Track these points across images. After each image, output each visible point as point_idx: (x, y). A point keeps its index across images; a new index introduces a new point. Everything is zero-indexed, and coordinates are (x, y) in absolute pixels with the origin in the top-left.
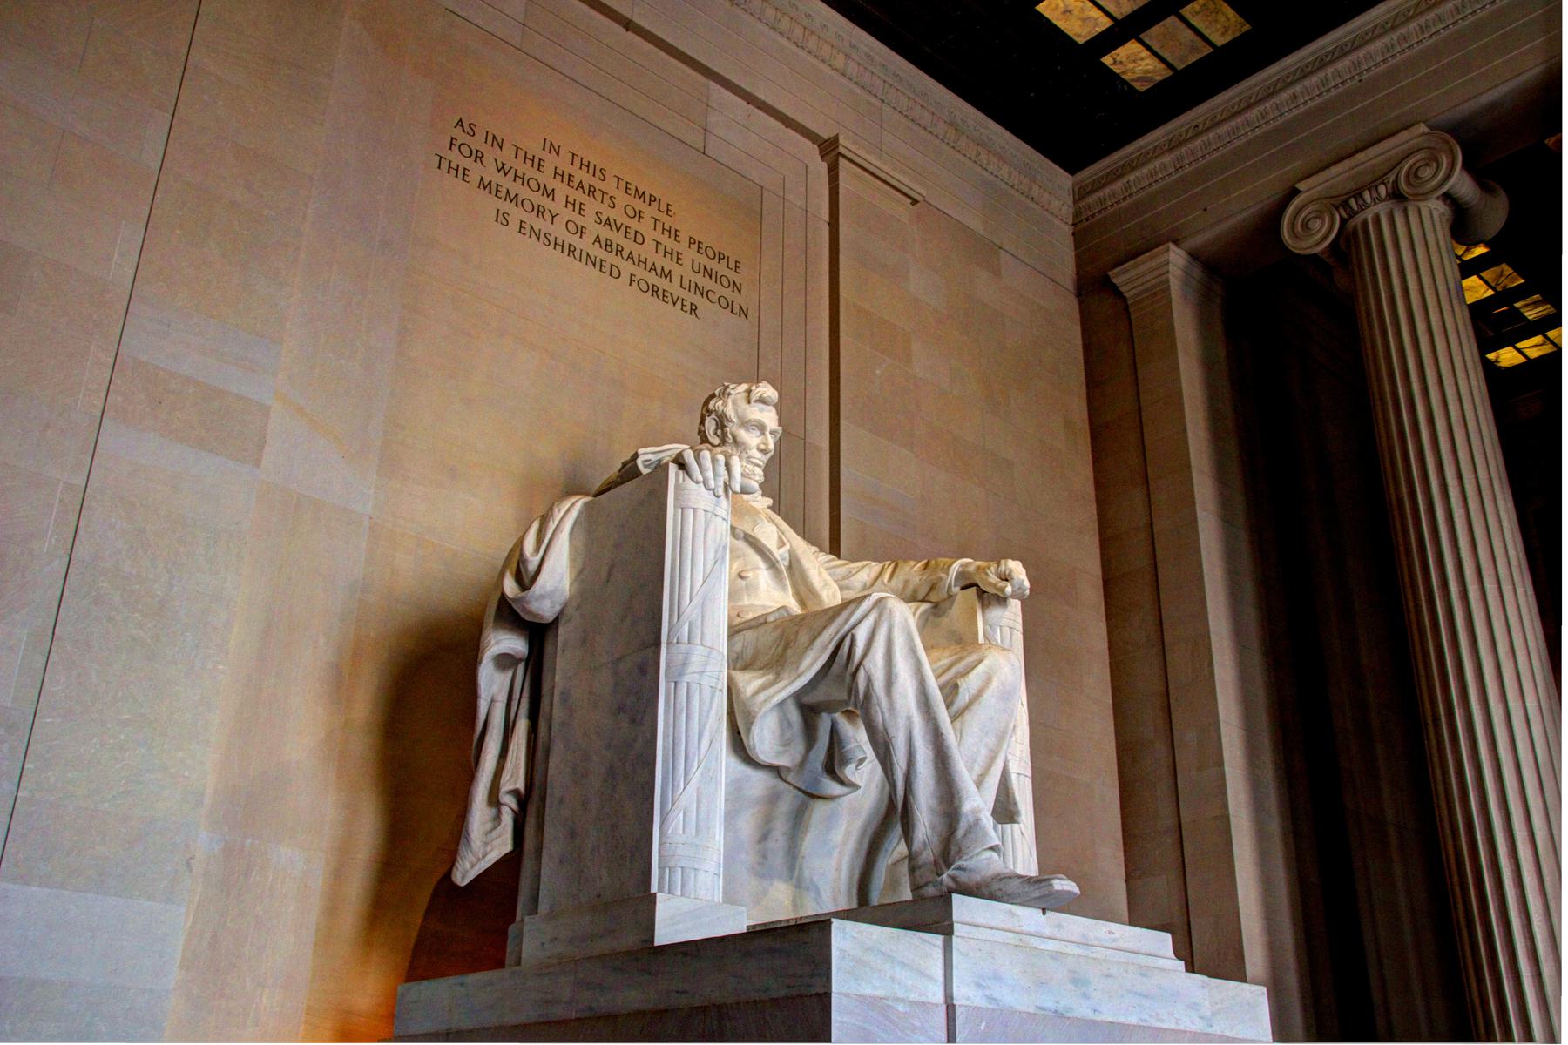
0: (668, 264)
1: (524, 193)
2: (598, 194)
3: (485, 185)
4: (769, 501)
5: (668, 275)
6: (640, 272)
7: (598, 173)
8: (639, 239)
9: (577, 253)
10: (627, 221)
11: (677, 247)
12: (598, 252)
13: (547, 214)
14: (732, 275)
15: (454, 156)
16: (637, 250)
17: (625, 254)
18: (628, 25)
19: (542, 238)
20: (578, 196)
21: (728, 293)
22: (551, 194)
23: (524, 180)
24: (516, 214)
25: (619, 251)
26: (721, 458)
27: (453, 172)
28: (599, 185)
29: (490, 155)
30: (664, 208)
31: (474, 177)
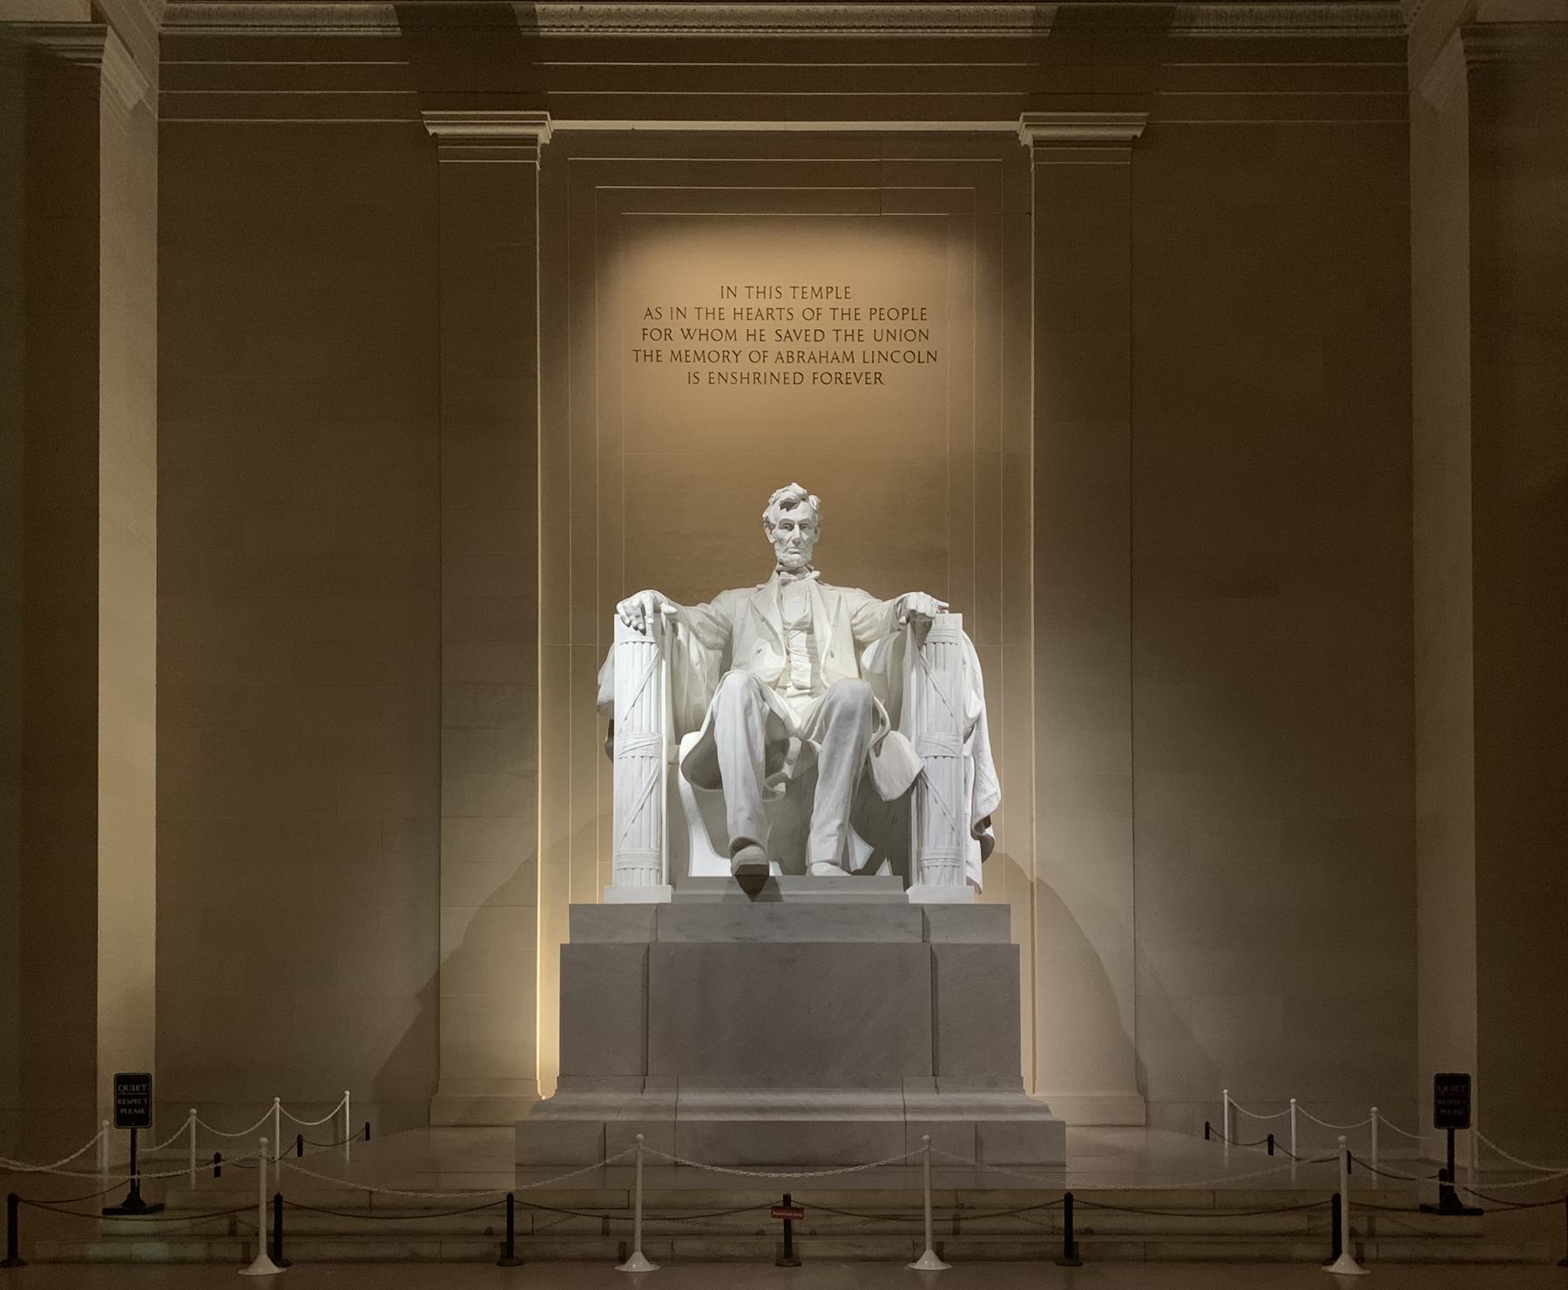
0: (850, 346)
1: (706, 346)
2: (776, 314)
5: (850, 357)
6: (822, 367)
9: (762, 379)
10: (805, 325)
11: (856, 325)
13: (732, 356)
14: (916, 326)
19: (730, 379)
20: (757, 324)
22: (731, 335)
24: (703, 368)
28: (774, 303)
30: (841, 294)
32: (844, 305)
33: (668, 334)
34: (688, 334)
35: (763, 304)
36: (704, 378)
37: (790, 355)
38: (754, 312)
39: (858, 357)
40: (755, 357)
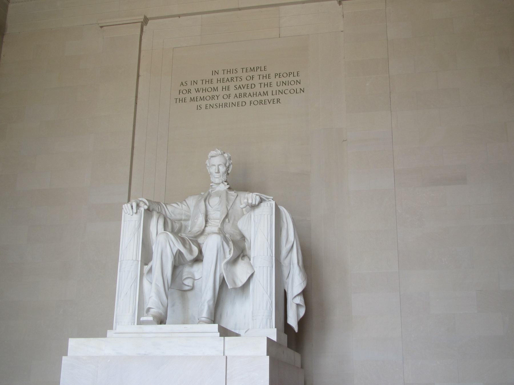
0: (266, 89)
2: (235, 79)
3: (192, 100)
4: (228, 186)
6: (253, 99)
7: (234, 71)
8: (253, 86)
9: (228, 105)
10: (247, 82)
11: (268, 81)
12: (236, 100)
14: (295, 79)
15: (182, 96)
16: (251, 91)
17: (247, 95)
18: (240, 9)
19: (214, 106)
20: (228, 84)
21: (295, 87)
22: (216, 89)
23: (206, 90)
24: (203, 103)
25: (245, 95)
26: (129, 205)
27: (181, 101)
28: (234, 75)
29: (193, 88)
30: (263, 69)
31: (188, 100)
32: (264, 73)
33: (189, 91)
34: (198, 91)
35: (229, 76)
36: (203, 107)
37: (240, 95)
38: (226, 79)
39: (270, 93)
40: (225, 97)
